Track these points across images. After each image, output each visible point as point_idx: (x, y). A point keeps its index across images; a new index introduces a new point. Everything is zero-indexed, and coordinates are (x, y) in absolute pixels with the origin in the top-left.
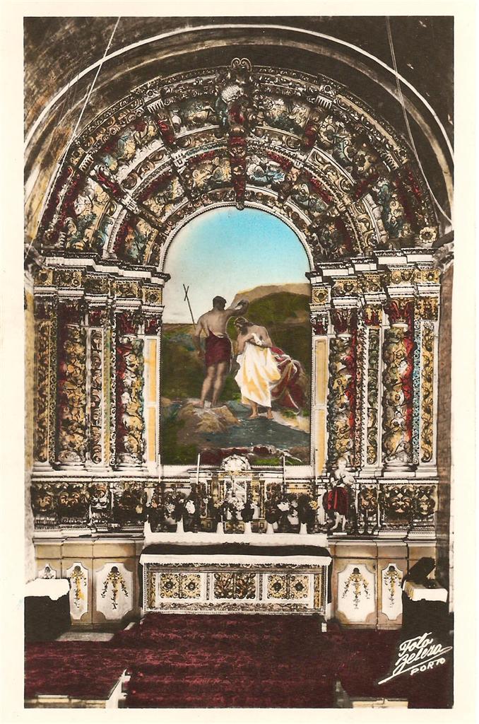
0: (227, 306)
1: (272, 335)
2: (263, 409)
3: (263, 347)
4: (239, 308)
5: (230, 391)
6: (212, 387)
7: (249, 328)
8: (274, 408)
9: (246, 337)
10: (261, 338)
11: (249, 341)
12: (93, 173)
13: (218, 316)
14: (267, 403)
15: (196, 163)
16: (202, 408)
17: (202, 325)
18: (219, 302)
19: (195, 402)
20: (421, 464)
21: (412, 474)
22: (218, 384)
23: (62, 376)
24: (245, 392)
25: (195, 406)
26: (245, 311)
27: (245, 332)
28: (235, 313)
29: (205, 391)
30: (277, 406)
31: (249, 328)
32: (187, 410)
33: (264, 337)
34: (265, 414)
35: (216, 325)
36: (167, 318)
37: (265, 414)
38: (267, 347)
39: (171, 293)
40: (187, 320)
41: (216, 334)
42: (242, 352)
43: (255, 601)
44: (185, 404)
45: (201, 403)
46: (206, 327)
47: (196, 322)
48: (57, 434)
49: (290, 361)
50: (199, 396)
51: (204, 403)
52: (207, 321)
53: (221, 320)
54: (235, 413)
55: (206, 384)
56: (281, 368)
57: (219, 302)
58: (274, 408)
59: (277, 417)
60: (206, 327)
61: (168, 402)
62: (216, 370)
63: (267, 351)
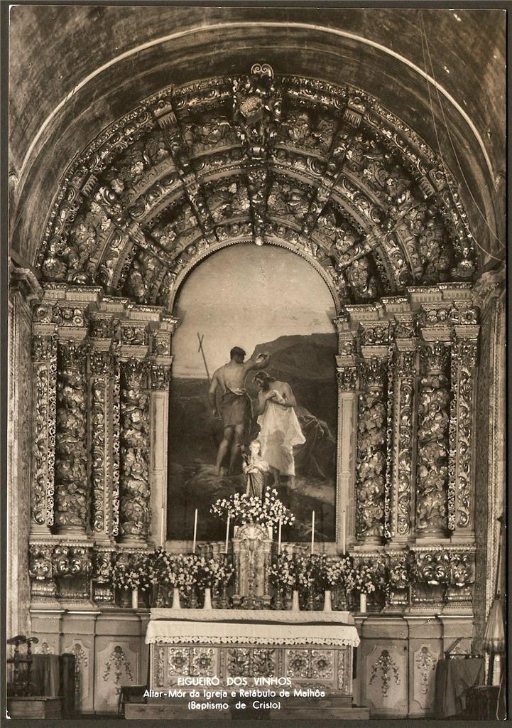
0: (247, 358)
1: (294, 391)
3: (287, 406)
9: (268, 395)
10: (284, 396)
11: (270, 399)
13: (236, 370)
18: (237, 354)
27: (266, 388)
32: (200, 478)
33: (287, 395)
35: (234, 377)
38: (291, 406)
42: (263, 411)
44: (198, 470)
45: (217, 470)
46: (223, 382)
47: (211, 377)
49: (316, 423)
52: (224, 375)
57: (237, 354)
63: (290, 411)
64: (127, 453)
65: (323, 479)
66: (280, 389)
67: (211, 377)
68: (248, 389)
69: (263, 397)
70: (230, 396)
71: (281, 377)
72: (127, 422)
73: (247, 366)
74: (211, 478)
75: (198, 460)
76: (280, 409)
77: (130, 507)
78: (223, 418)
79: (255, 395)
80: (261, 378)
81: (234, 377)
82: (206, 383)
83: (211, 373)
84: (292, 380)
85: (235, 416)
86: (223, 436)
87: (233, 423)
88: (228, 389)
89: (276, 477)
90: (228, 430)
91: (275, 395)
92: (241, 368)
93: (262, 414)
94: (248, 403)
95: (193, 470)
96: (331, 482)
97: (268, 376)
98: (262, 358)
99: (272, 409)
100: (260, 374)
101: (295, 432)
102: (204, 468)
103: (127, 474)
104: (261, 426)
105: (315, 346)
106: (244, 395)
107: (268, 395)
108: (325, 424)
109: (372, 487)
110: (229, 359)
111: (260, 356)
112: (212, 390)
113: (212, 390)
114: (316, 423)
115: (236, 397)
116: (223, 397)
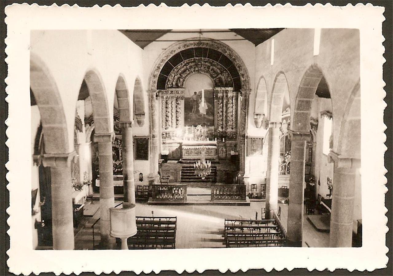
0: (197, 94)
2: (205, 115)
5: (198, 111)
6: (194, 109)
8: (206, 115)
14: (205, 114)
15: (191, 67)
18: (195, 93)
19: (191, 113)
22: (195, 110)
24: (200, 111)
29: (193, 112)
30: (207, 113)
36: (186, 96)
39: (186, 91)
40: (190, 97)
41: (195, 100)
50: (191, 112)
54: (199, 116)
56: (208, 106)
57: (195, 93)
59: (206, 116)
61: (186, 113)
62: (195, 107)
75: (189, 112)
82: (190, 98)
83: (191, 97)
90: (194, 107)
106: (197, 100)
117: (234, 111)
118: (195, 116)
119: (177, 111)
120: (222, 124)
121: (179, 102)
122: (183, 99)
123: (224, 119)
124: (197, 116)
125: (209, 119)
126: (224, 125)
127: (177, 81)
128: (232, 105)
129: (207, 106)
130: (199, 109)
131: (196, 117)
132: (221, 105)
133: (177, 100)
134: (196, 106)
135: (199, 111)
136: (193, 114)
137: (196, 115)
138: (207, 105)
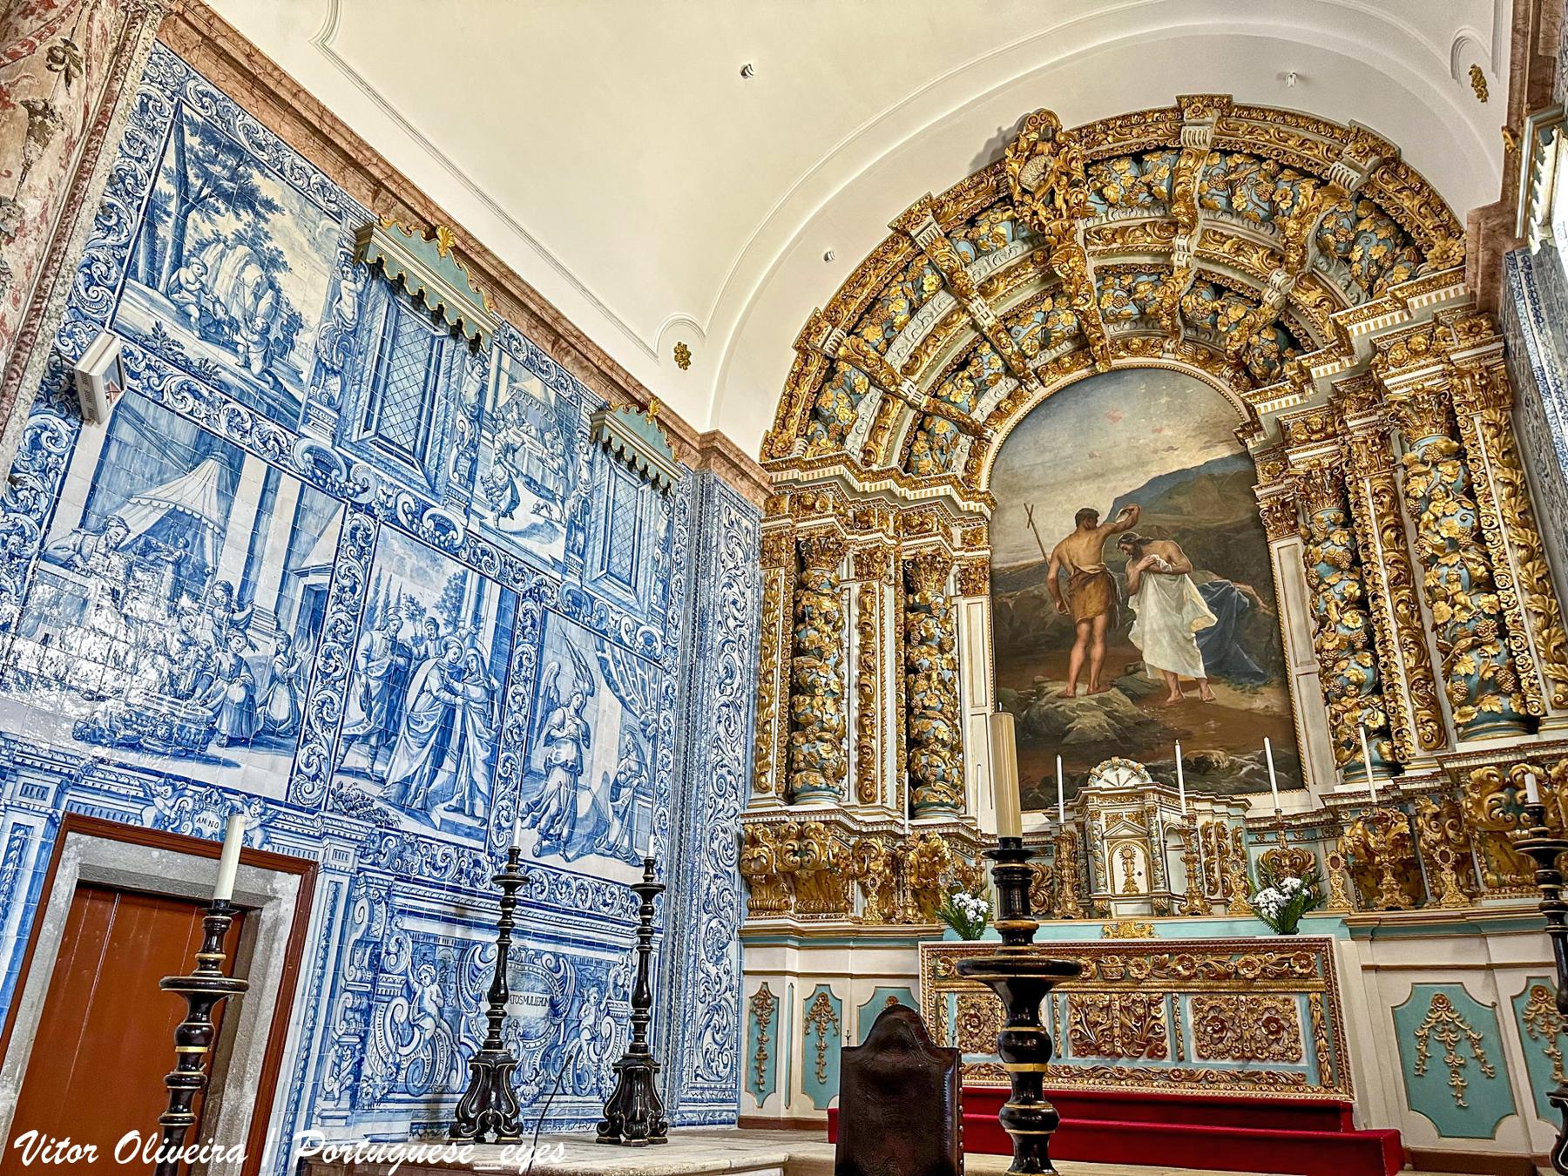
0: (1101, 520)
1: (1185, 550)
2: (1194, 684)
3: (1177, 573)
4: (1123, 519)
6: (1087, 659)
7: (1144, 548)
9: (1142, 564)
10: (1169, 560)
11: (1147, 569)
12: (842, 351)
13: (1086, 540)
14: (1201, 672)
16: (1074, 697)
17: (1060, 560)
18: (1086, 518)
19: (1058, 688)
20: (1552, 714)
21: (1533, 739)
22: (1097, 651)
23: (798, 651)
25: (1060, 696)
26: (1134, 522)
27: (1137, 555)
28: (1115, 531)
29: (1073, 674)
31: (1144, 548)
32: (1045, 705)
33: (1175, 557)
34: (1196, 694)
35: (1084, 552)
37: (1196, 694)
38: (1184, 573)
42: (1138, 589)
43: (1168, 1063)
44: (1040, 693)
45: (1071, 689)
46: (1067, 561)
47: (1049, 557)
48: (790, 747)
49: (1233, 590)
50: (1064, 676)
51: (1075, 688)
52: (1068, 551)
53: (1092, 543)
54: (1136, 698)
55: (1077, 655)
57: (1086, 518)
58: (1209, 681)
59: (1221, 694)
60: (1067, 561)
62: (1092, 627)
63: (1183, 581)
64: (916, 681)
65: (1256, 676)
66: (1160, 552)
67: (1049, 557)
68: (1109, 562)
69: (1133, 571)
70: (1080, 577)
71: (1161, 534)
72: (916, 636)
73: (1103, 531)
74: (1065, 701)
75: (1039, 678)
76: (1163, 579)
77: (924, 760)
78: (1073, 612)
79: (1121, 567)
80: (1127, 543)
81: (1084, 552)
82: (1043, 567)
83: (1049, 551)
84: (1182, 536)
85: (1092, 602)
86: (1076, 636)
87: (1089, 615)
88: (1076, 568)
89: (1173, 686)
90: (1084, 628)
91: (1155, 562)
92: (1093, 535)
93: (1135, 593)
94: (1110, 583)
95: (1033, 694)
96: (1276, 679)
97: (1138, 537)
98: (1126, 515)
99: (1151, 584)
100: (1124, 537)
101: (1196, 608)
102: (1050, 689)
103: (917, 711)
104: (1137, 611)
105: (1212, 477)
106: (1104, 572)
107: (1142, 564)
108: (1249, 589)
109: (1355, 669)
110: (1075, 527)
111: (1123, 513)
112: (1052, 575)
113: (1052, 575)
114: (1233, 590)
115: (1090, 577)
116: (1070, 580)
117: (1499, 506)
118: (1102, 701)
119: (911, 669)
120: (1384, 733)
121: (929, 592)
122: (976, 592)
123: (1401, 662)
124: (1122, 703)
125: (1249, 711)
126: (1410, 725)
127: (909, 446)
128: (1449, 471)
129: (1210, 604)
130: (1138, 645)
131: (1109, 714)
132: (1339, 537)
133: (910, 589)
134: (1100, 621)
135: (1138, 655)
136: (1082, 689)
137: (1114, 692)
138: (1203, 590)
